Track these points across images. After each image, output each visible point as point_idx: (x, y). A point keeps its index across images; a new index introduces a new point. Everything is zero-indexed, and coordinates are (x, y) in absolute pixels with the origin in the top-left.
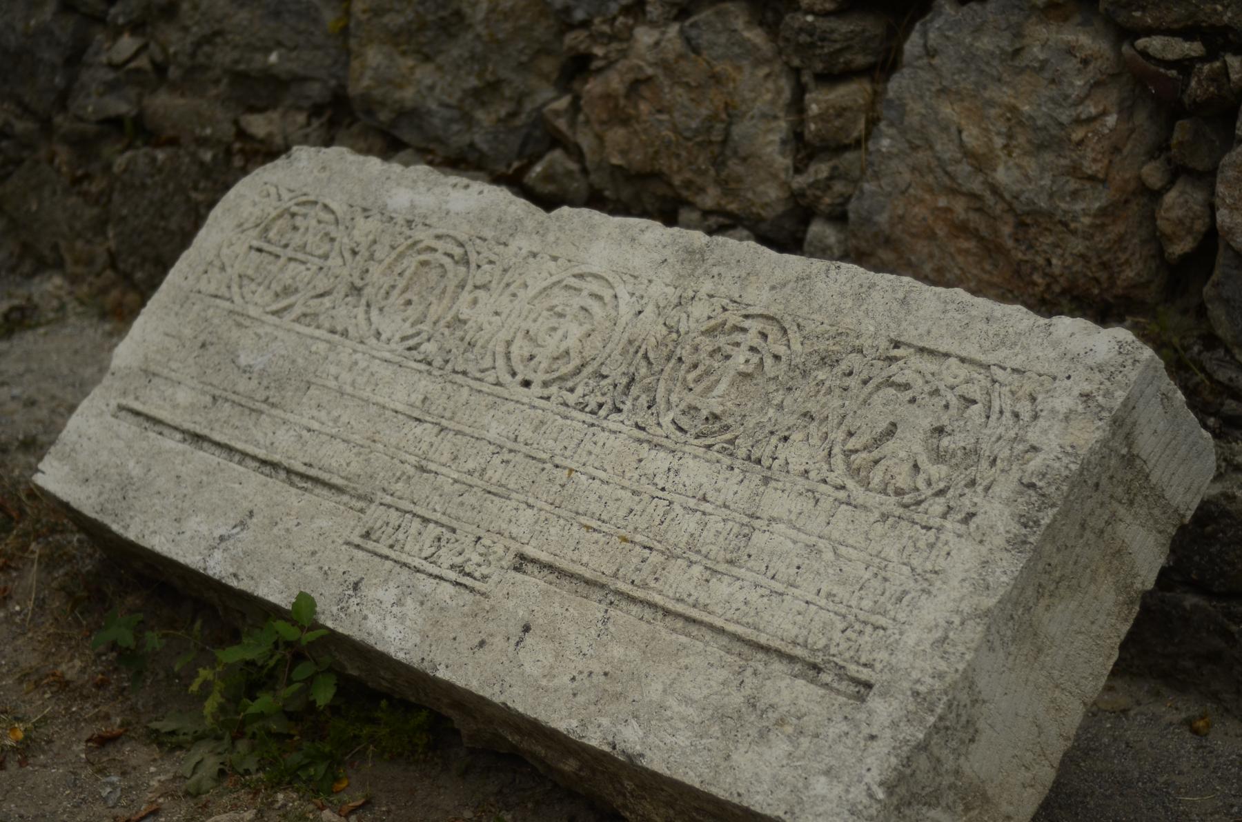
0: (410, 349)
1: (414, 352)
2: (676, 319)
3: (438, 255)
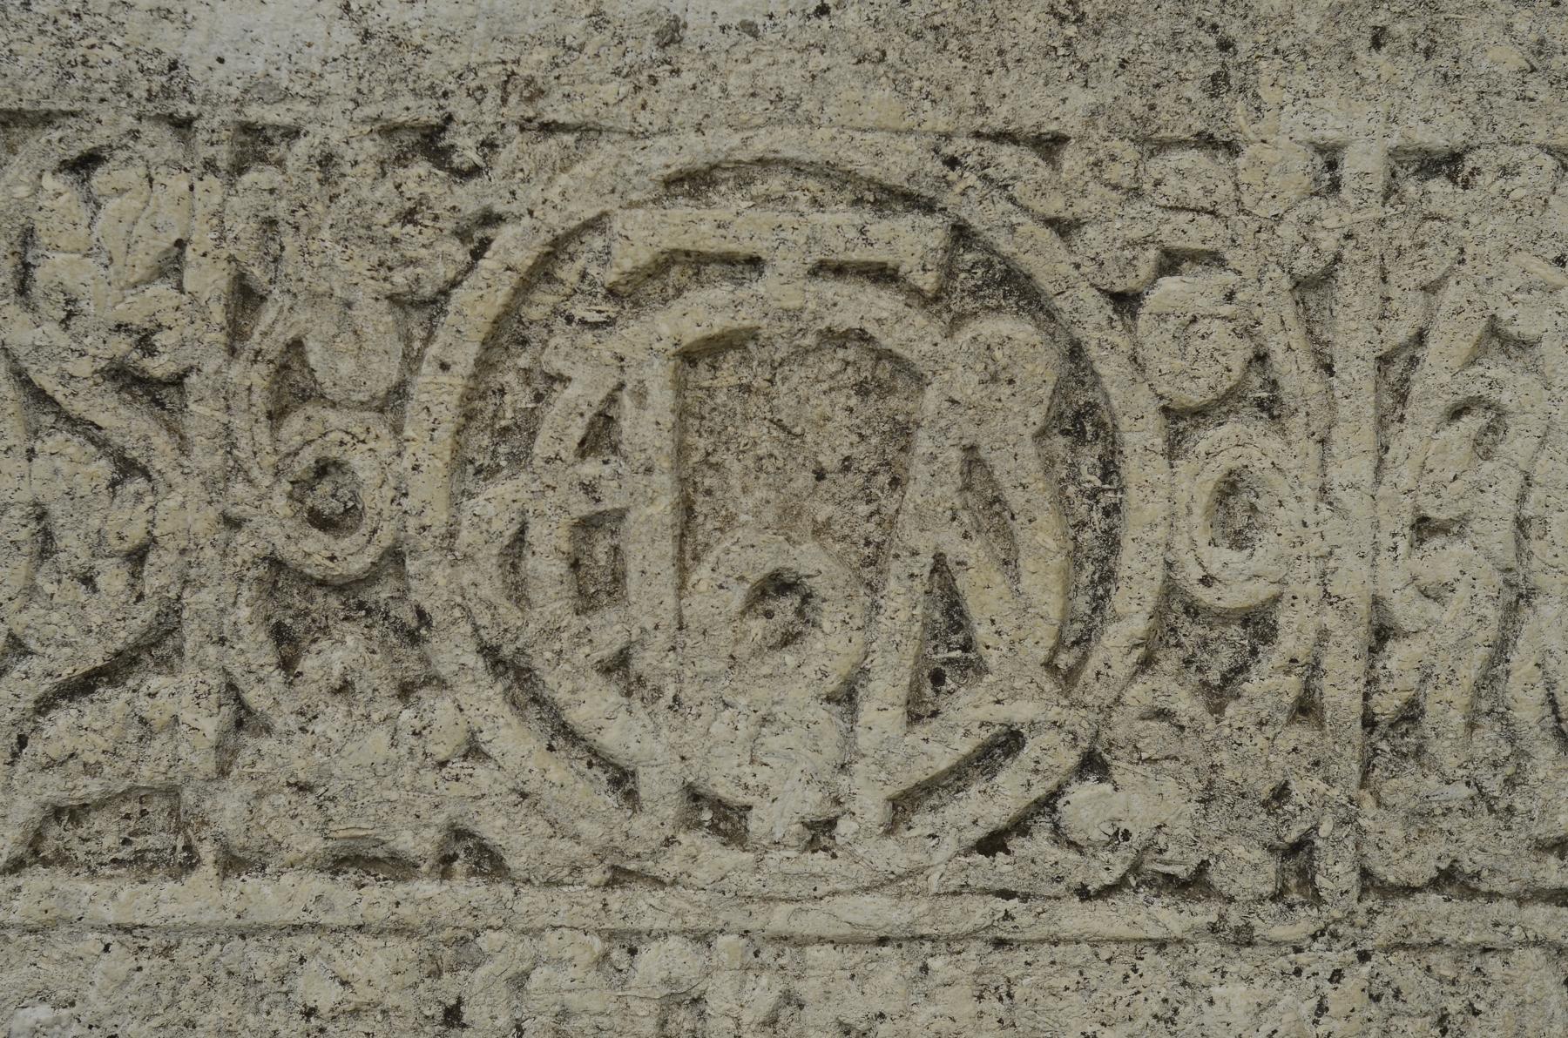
0: (992, 844)
1: (1038, 845)
3: (780, 288)
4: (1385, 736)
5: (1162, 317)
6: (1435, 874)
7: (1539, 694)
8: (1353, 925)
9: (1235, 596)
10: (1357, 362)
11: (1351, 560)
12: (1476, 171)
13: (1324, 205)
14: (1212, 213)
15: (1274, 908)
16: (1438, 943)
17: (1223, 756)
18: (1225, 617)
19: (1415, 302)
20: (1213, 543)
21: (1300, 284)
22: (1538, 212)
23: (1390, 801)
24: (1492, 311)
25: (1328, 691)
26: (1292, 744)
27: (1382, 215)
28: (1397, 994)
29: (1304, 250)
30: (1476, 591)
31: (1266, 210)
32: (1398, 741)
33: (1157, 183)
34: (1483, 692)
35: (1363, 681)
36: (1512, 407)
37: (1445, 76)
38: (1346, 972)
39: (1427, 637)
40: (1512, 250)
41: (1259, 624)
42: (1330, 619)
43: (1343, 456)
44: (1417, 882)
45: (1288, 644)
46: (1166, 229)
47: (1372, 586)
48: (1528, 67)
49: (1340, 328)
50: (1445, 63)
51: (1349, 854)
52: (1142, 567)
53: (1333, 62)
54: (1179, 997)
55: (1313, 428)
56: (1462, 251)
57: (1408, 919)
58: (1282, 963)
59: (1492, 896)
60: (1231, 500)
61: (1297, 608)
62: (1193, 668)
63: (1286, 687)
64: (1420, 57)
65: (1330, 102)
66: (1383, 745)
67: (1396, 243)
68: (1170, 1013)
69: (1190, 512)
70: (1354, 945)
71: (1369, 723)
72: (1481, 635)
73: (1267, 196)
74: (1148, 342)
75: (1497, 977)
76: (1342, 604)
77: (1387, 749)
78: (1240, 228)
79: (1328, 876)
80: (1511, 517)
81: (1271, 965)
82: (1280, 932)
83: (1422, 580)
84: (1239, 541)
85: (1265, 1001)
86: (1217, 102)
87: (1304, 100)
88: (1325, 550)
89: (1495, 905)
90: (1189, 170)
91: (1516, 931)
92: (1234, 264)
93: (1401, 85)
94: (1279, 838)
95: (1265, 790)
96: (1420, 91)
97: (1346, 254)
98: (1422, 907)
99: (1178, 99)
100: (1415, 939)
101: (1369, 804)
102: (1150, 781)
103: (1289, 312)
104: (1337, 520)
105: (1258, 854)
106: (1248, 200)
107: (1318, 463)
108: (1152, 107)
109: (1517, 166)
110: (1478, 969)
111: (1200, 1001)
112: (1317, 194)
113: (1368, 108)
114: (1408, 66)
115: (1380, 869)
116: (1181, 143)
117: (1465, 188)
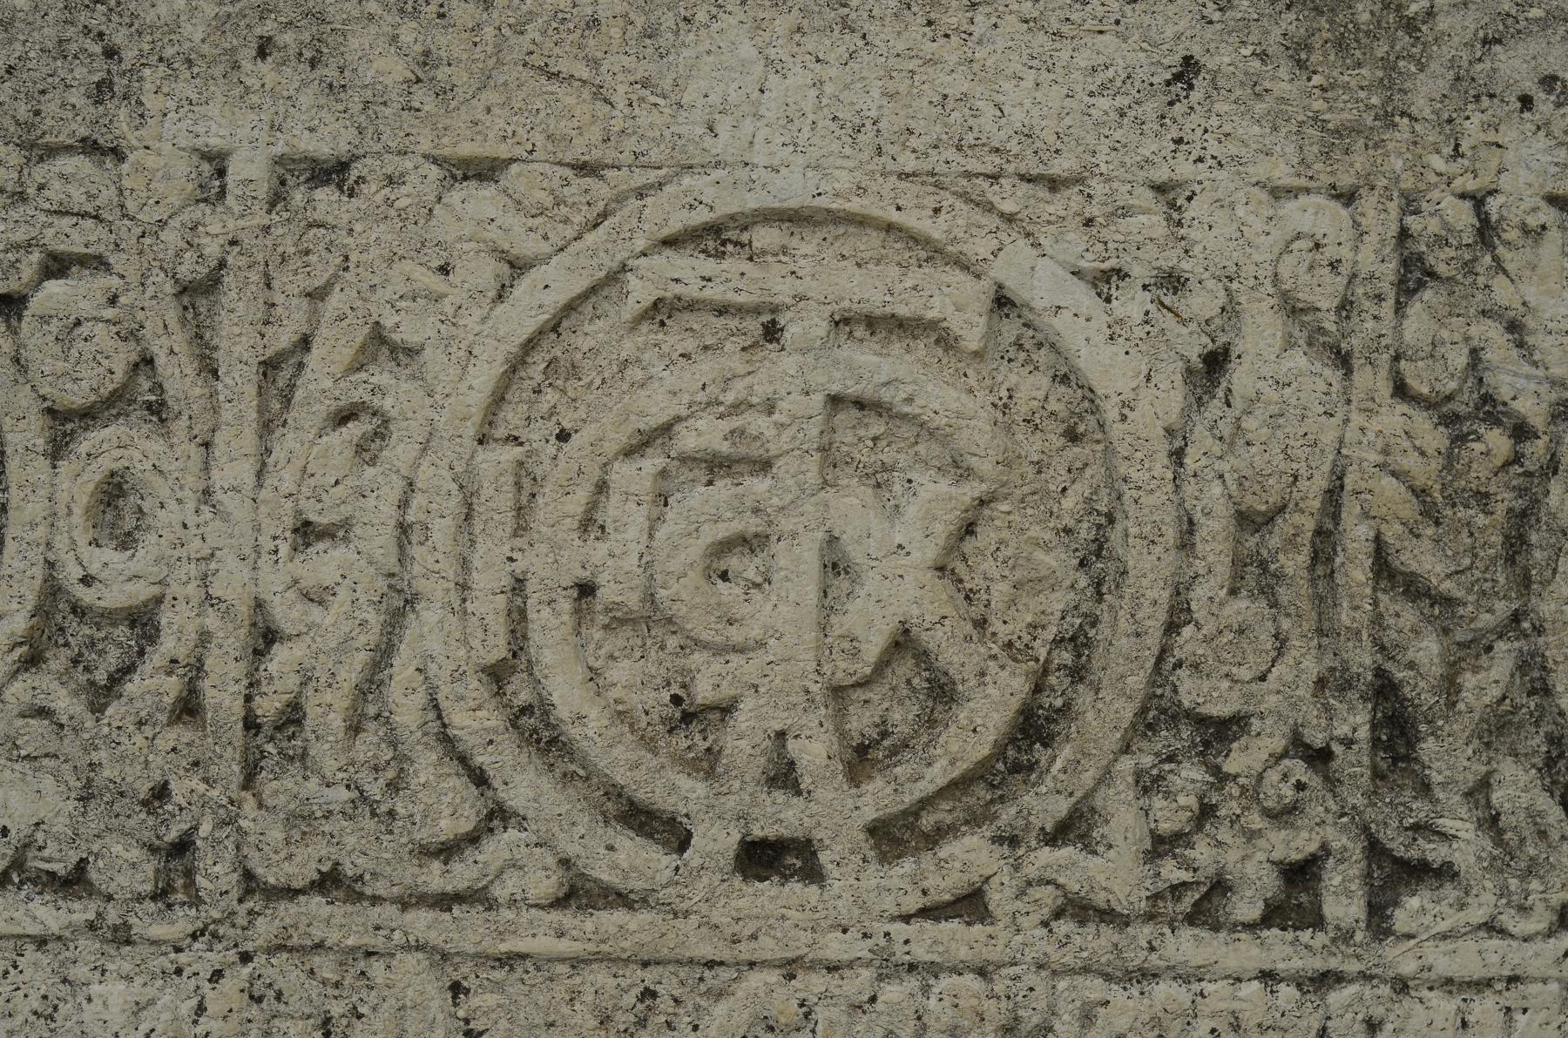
2: (1459, 359)
4: (272, 739)
5: (44, 319)
6: (316, 876)
7: (420, 698)
8: (234, 926)
9: (115, 596)
10: (240, 366)
11: (231, 562)
12: (361, 180)
13: (208, 211)
14: (96, 217)
15: (150, 906)
16: (319, 946)
17: (102, 755)
18: (109, 617)
19: (299, 308)
20: (95, 543)
21: (186, 290)
22: (422, 221)
23: (270, 802)
24: (375, 317)
25: (210, 692)
26: (172, 744)
27: (266, 222)
28: (279, 996)
29: (188, 255)
30: (357, 595)
31: (149, 216)
32: (285, 744)
33: (41, 187)
34: (370, 697)
35: (245, 682)
36: (394, 413)
37: (331, 86)
38: (227, 973)
39: (308, 640)
40: (396, 258)
41: (143, 621)
42: (212, 621)
43: (224, 459)
44: (297, 884)
45: (168, 645)
46: (50, 232)
47: (253, 588)
48: (413, 78)
49: (224, 333)
50: (331, 73)
51: (229, 854)
52: (22, 565)
53: (217, 71)
54: (60, 995)
55: (195, 432)
56: (347, 258)
57: (288, 921)
58: (164, 962)
59: (376, 900)
60: (121, 502)
61: (177, 608)
62: (80, 668)
63: (166, 687)
64: (306, 67)
65: (213, 110)
66: (270, 748)
67: (280, 250)
68: (50, 1010)
69: (70, 513)
70: (236, 946)
71: (251, 724)
72: (363, 639)
73: (151, 201)
74: (31, 343)
75: (379, 980)
76: (223, 606)
77: (275, 752)
78: (124, 233)
79: (207, 876)
80: (393, 522)
81: (151, 964)
82: (158, 931)
83: (303, 584)
84: (126, 542)
85: (143, 1000)
86: (101, 108)
87: (187, 108)
88: (206, 552)
89: (378, 909)
90: (73, 175)
91: (397, 935)
92: (118, 268)
93: (285, 93)
94: (158, 837)
95: (144, 789)
96: (305, 100)
97: (230, 260)
98: (303, 909)
99: (63, 105)
100: (295, 941)
101: (249, 805)
102: (29, 778)
103: (172, 316)
104: (218, 523)
105: (135, 854)
106: (131, 206)
107: (200, 465)
108: (37, 113)
109: (402, 175)
110: (363, 973)
111: (81, 999)
112: (205, 200)
113: (252, 116)
114: (293, 76)
115: (260, 871)
116: (68, 149)
117: (350, 196)
